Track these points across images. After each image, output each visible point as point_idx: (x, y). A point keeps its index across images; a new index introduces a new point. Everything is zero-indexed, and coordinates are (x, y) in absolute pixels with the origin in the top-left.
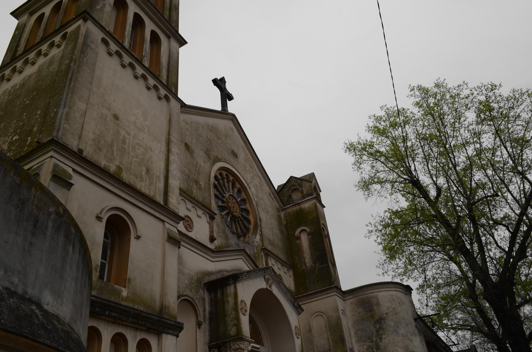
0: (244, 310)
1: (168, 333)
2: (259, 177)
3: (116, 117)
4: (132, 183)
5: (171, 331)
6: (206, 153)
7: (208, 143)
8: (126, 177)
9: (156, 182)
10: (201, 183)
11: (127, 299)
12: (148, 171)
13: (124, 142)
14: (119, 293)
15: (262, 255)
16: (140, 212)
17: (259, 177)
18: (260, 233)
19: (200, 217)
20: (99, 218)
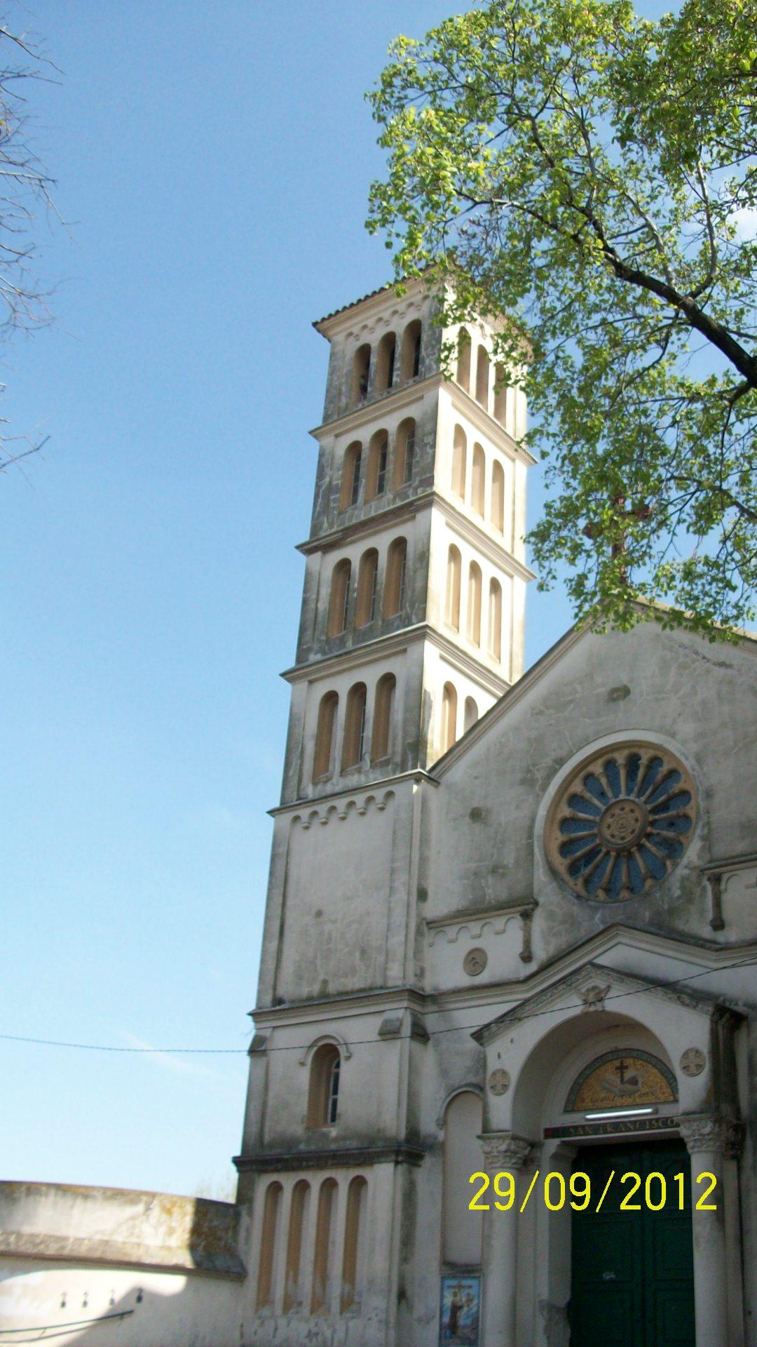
0: (499, 1087)
1: (380, 1163)
2: (722, 664)
3: (319, 914)
4: (341, 989)
5: (383, 1159)
6: (523, 782)
7: (532, 752)
8: (332, 988)
9: (376, 958)
10: (505, 862)
11: (336, 1139)
12: (363, 952)
13: (330, 939)
14: (326, 1135)
15: (704, 889)
16: (351, 1022)
17: (722, 664)
18: (706, 831)
19: (503, 932)
20: (302, 1064)
